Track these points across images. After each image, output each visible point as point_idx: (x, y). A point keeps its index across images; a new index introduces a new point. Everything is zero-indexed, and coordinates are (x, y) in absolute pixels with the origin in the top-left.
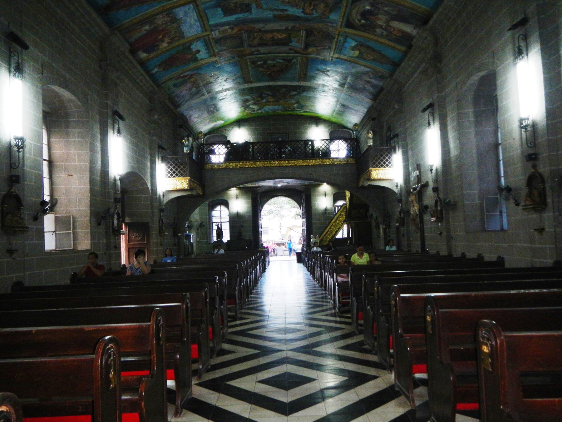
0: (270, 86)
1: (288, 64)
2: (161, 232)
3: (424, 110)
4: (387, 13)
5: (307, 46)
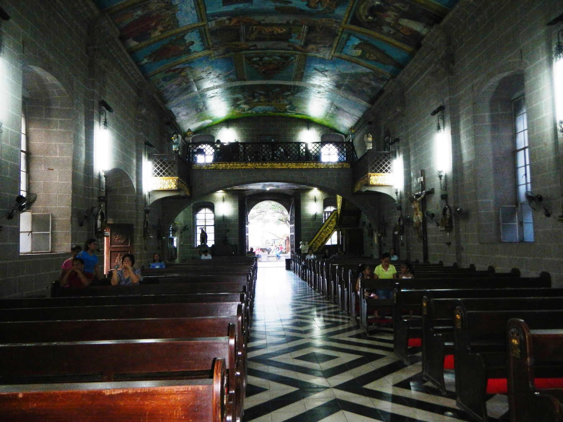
2: (145, 234)
3: (434, 113)
4: (397, 9)
5: (306, 44)
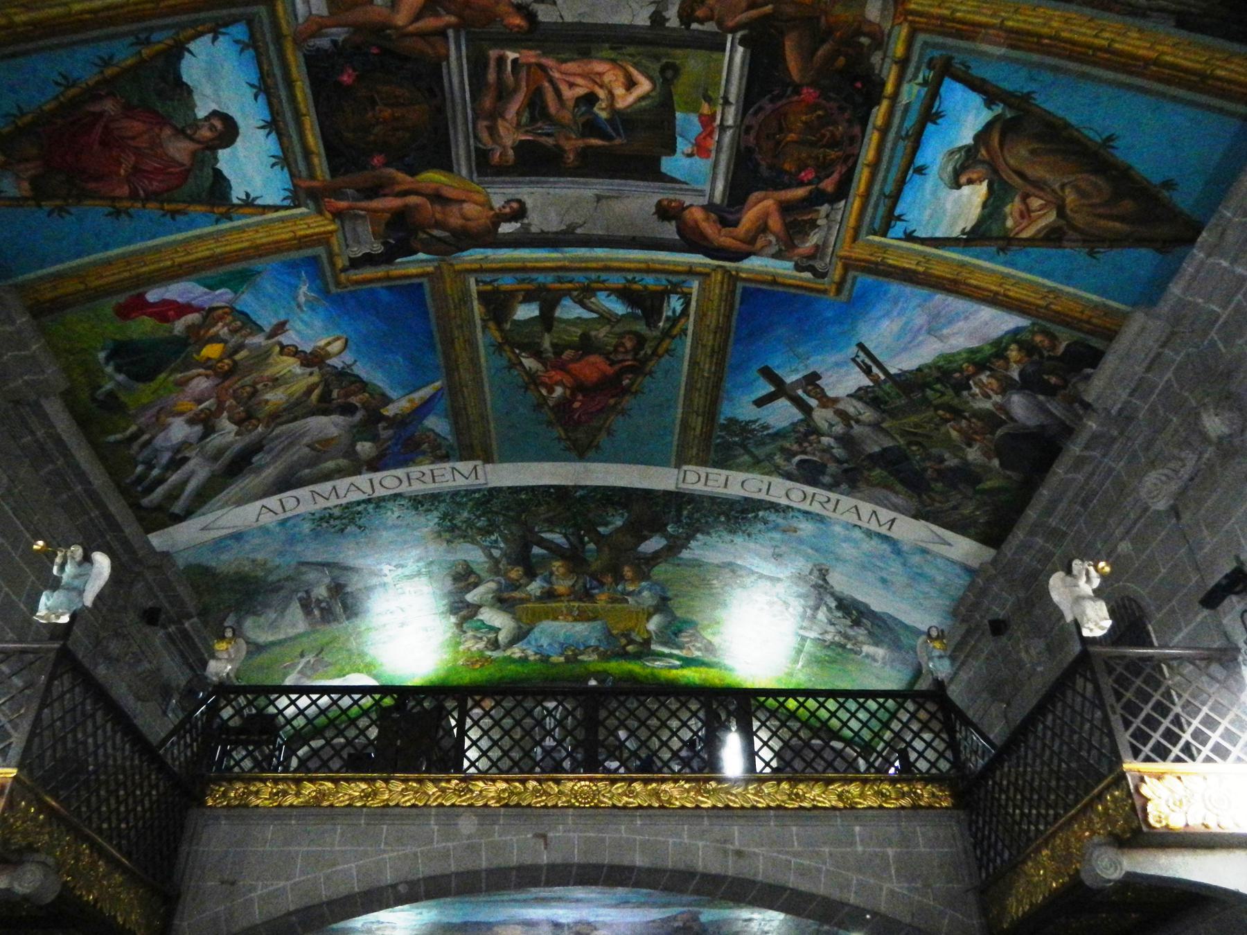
0: (561, 494)
1: (641, 327)
